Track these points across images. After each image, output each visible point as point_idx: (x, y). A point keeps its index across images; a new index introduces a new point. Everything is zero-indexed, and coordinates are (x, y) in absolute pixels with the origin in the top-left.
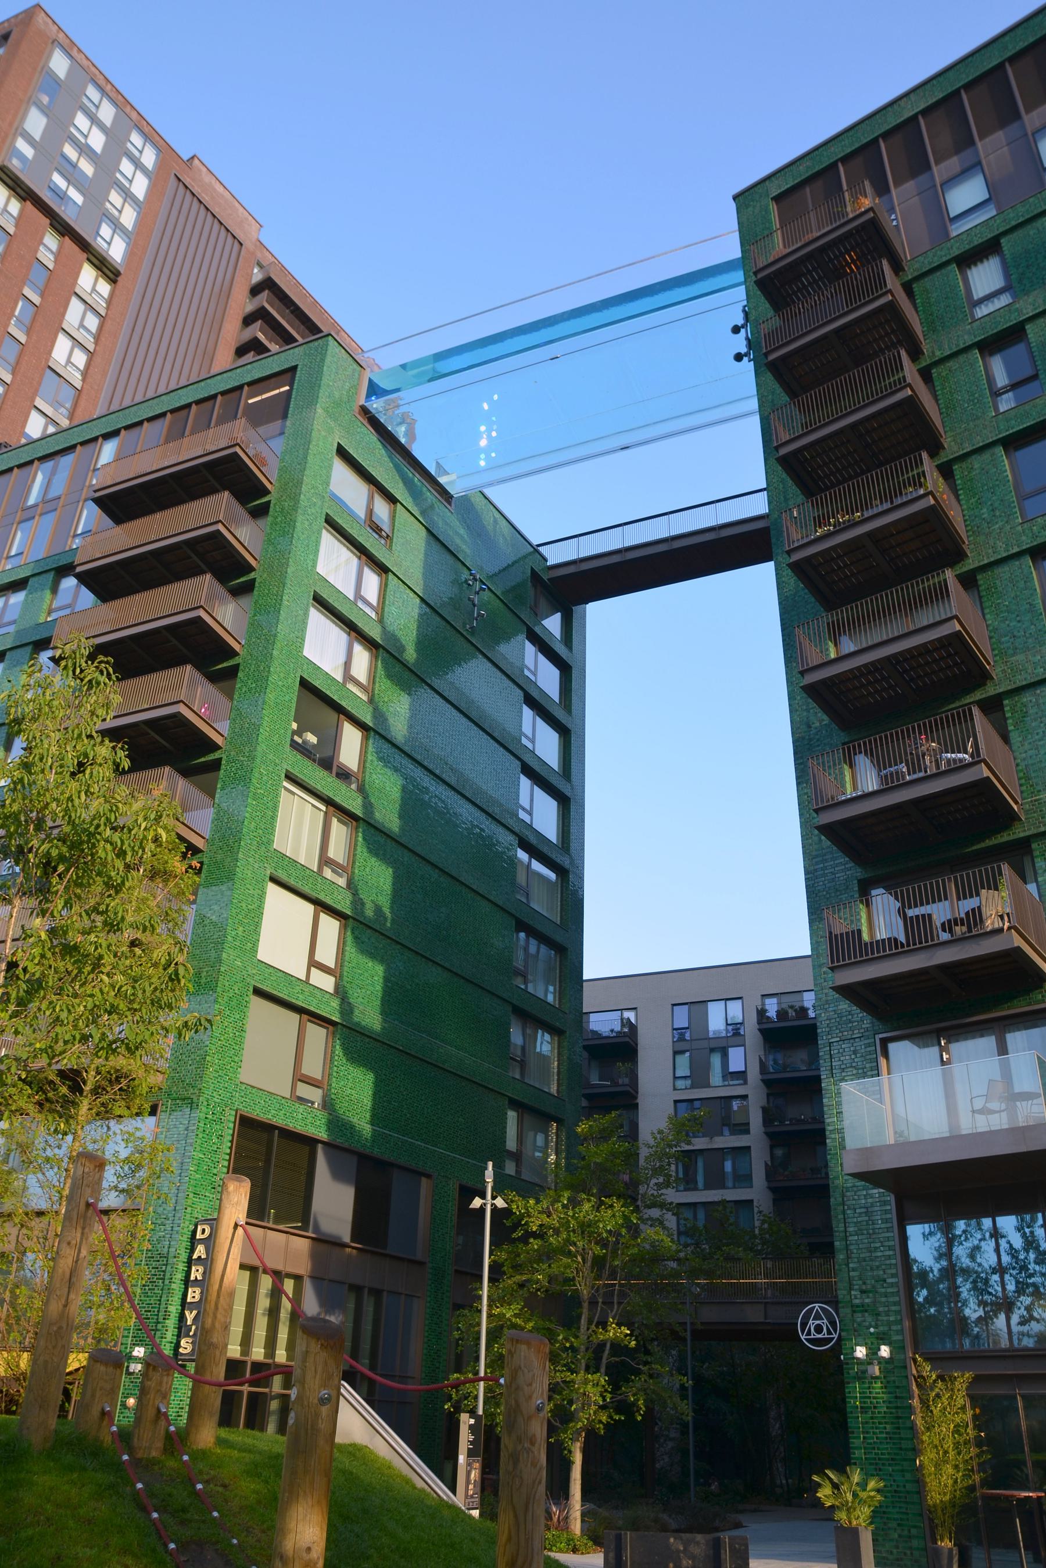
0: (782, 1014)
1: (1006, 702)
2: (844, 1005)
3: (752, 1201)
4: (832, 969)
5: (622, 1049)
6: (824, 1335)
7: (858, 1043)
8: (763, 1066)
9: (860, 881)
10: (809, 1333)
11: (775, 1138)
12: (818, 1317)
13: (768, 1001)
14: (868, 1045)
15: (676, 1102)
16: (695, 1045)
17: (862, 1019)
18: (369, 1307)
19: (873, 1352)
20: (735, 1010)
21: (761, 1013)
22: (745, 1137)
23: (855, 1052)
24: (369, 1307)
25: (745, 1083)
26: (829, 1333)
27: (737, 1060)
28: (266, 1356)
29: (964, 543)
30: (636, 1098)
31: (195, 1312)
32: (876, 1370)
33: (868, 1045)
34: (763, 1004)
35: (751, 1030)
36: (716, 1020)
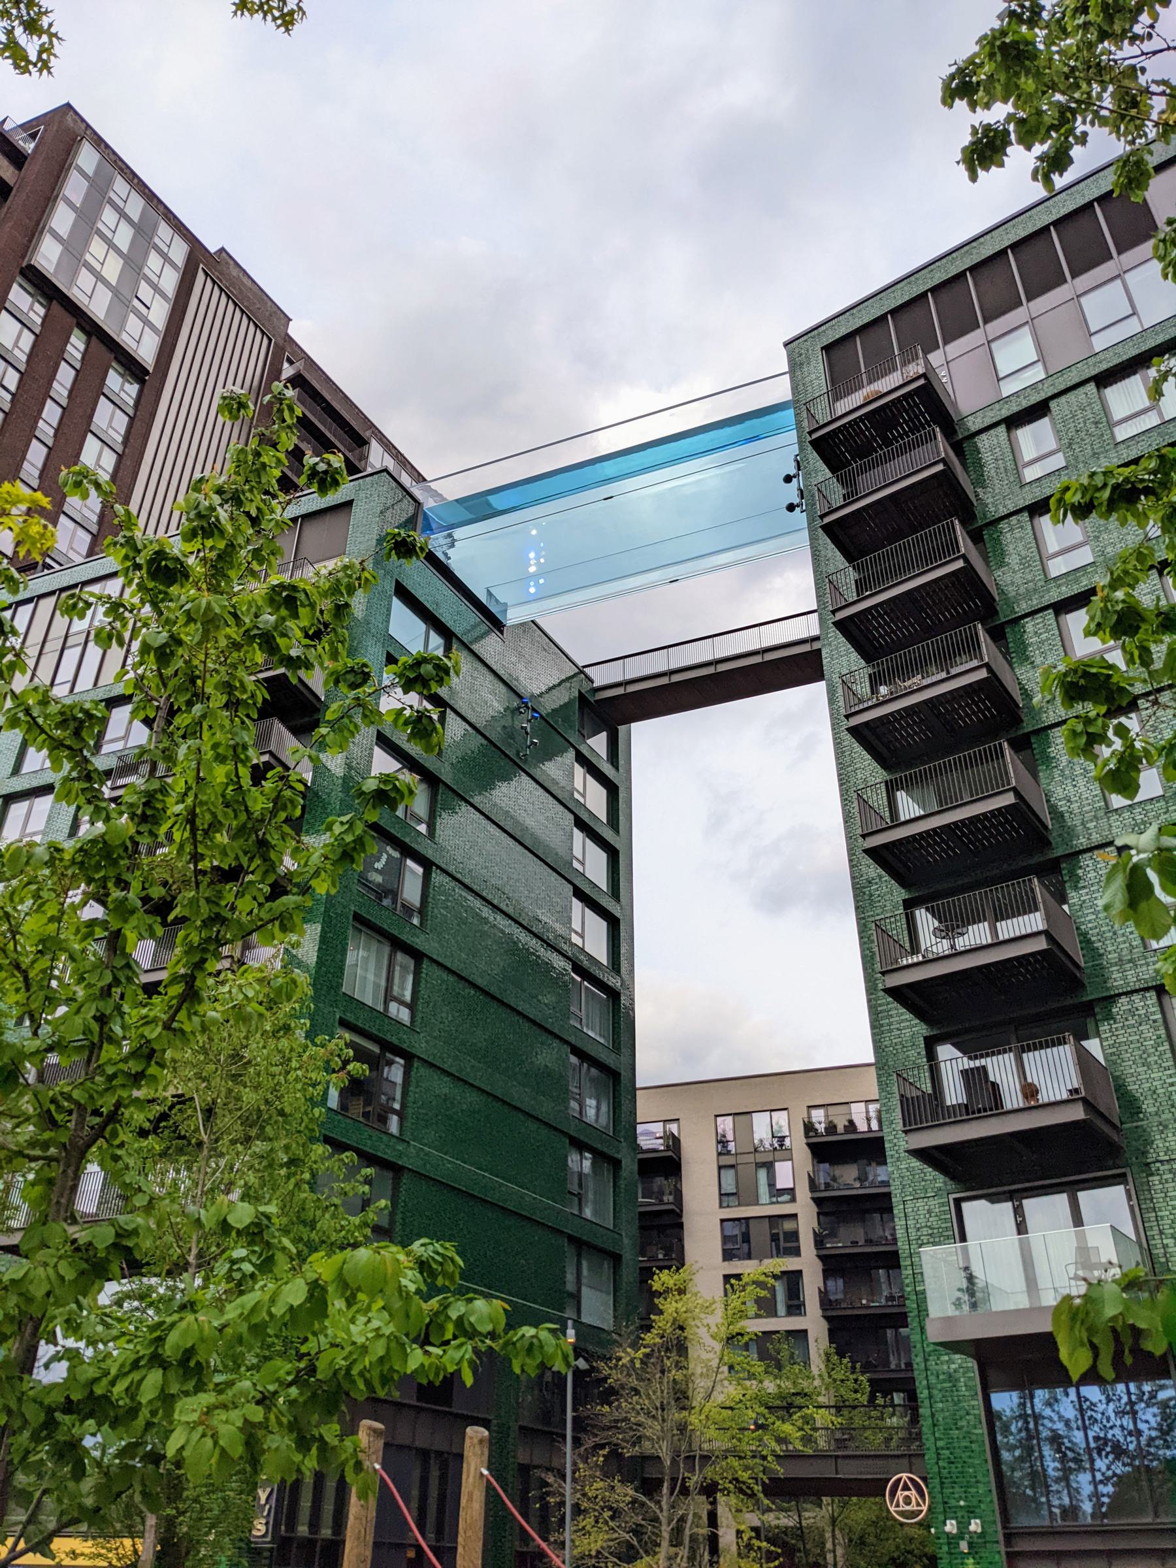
0: (831, 1128)
1: (1063, 865)
2: (916, 1163)
3: (806, 1331)
4: (906, 1132)
5: (667, 1165)
6: (913, 1507)
7: (932, 1202)
8: (813, 1186)
9: (925, 1038)
10: (898, 1505)
11: (832, 1265)
12: (906, 1488)
13: (814, 1113)
14: (942, 1205)
15: (722, 1221)
16: (743, 1166)
17: (936, 1179)
18: (435, 1473)
19: (963, 1525)
20: (781, 1118)
21: (809, 1128)
22: (796, 1259)
23: (929, 1211)
24: (435, 1473)
25: (793, 1200)
26: (918, 1505)
27: (784, 1175)
28: (334, 1534)
29: (1046, 828)
30: (680, 1216)
31: (268, 1490)
32: (964, 1546)
33: (942, 1205)
34: (809, 1117)
35: (798, 1143)
36: (761, 1129)
